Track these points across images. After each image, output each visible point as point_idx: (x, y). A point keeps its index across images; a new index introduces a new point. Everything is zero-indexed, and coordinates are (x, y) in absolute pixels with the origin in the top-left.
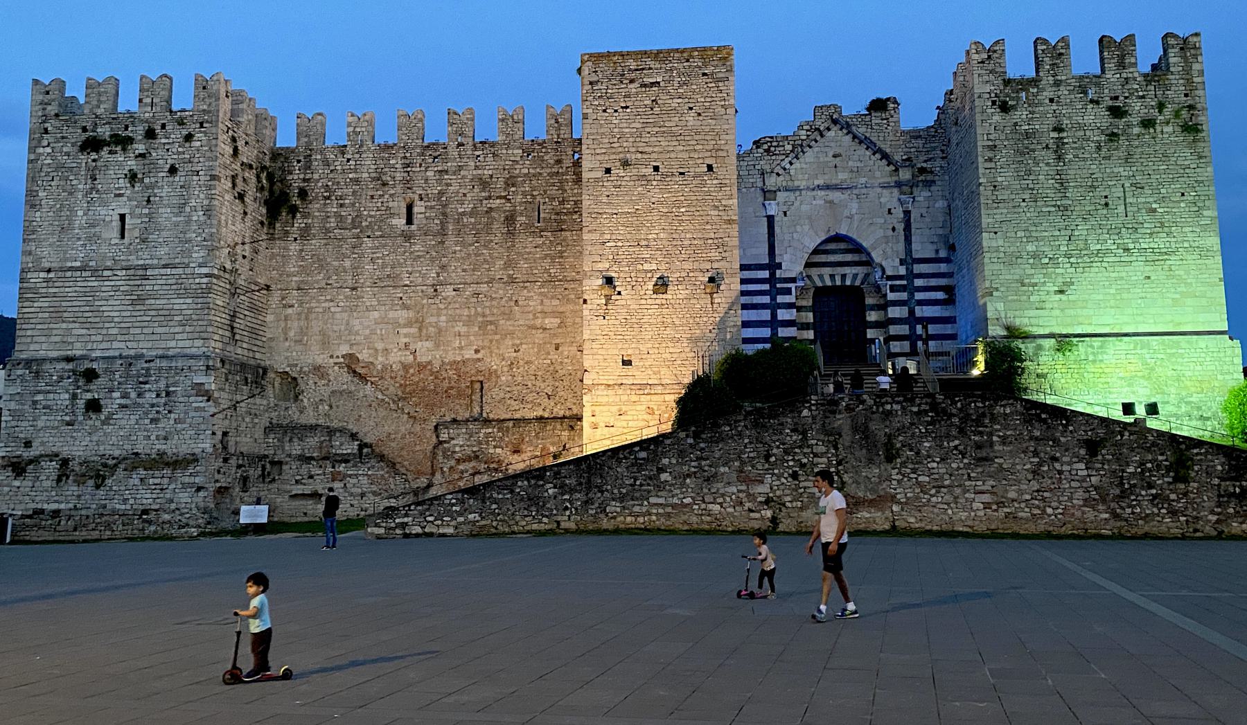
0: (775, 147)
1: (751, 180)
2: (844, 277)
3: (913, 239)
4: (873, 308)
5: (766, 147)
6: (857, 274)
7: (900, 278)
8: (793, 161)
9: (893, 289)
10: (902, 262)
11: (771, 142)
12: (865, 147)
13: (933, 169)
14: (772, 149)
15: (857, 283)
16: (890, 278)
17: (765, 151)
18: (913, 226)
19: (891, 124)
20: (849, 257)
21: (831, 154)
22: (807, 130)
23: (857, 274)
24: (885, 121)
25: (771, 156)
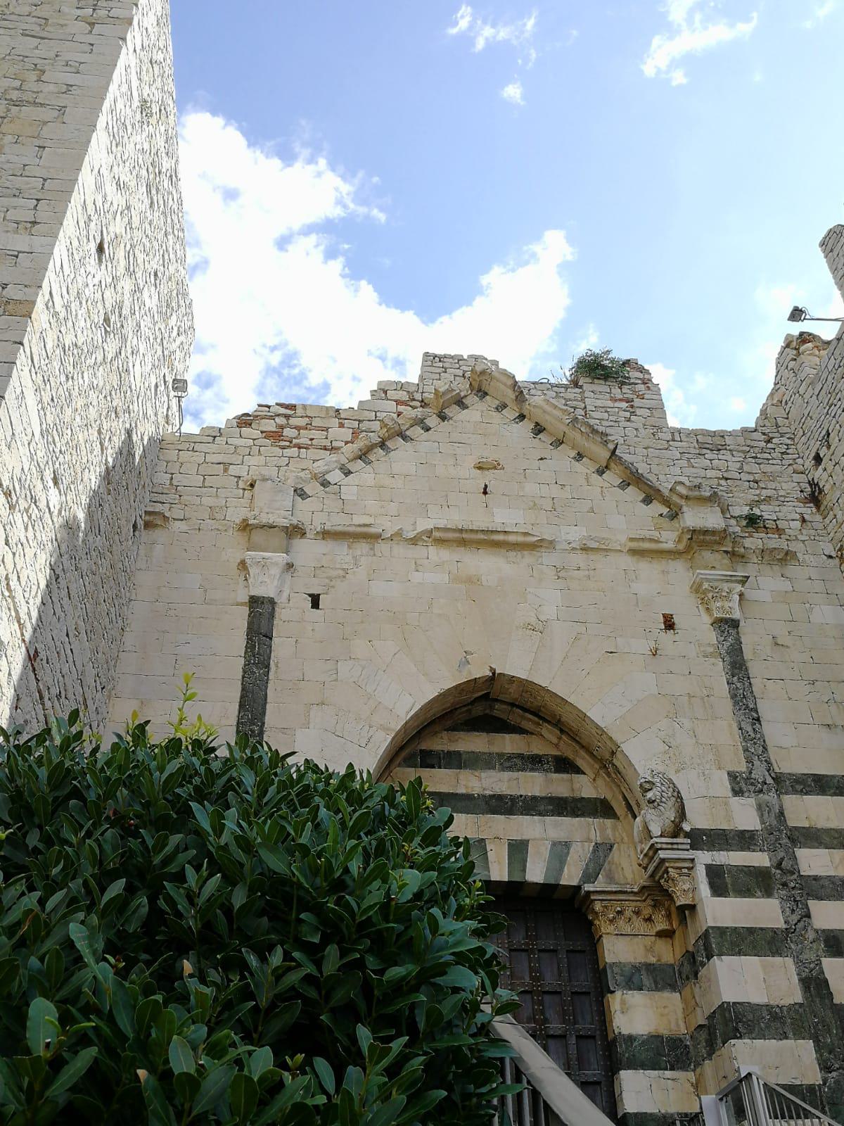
0: (298, 428)
1: (207, 501)
2: (518, 850)
3: (764, 709)
4: (637, 977)
5: (270, 426)
6: (567, 845)
7: (745, 840)
8: (350, 466)
9: (720, 881)
10: (739, 784)
11: (287, 417)
12: (573, 453)
13: (781, 524)
14: (288, 432)
15: (570, 876)
16: (699, 839)
17: (267, 435)
18: (755, 669)
19: (638, 412)
20: (533, 784)
21: (471, 461)
22: (398, 402)
23: (567, 845)
24: (624, 405)
25: (283, 448)
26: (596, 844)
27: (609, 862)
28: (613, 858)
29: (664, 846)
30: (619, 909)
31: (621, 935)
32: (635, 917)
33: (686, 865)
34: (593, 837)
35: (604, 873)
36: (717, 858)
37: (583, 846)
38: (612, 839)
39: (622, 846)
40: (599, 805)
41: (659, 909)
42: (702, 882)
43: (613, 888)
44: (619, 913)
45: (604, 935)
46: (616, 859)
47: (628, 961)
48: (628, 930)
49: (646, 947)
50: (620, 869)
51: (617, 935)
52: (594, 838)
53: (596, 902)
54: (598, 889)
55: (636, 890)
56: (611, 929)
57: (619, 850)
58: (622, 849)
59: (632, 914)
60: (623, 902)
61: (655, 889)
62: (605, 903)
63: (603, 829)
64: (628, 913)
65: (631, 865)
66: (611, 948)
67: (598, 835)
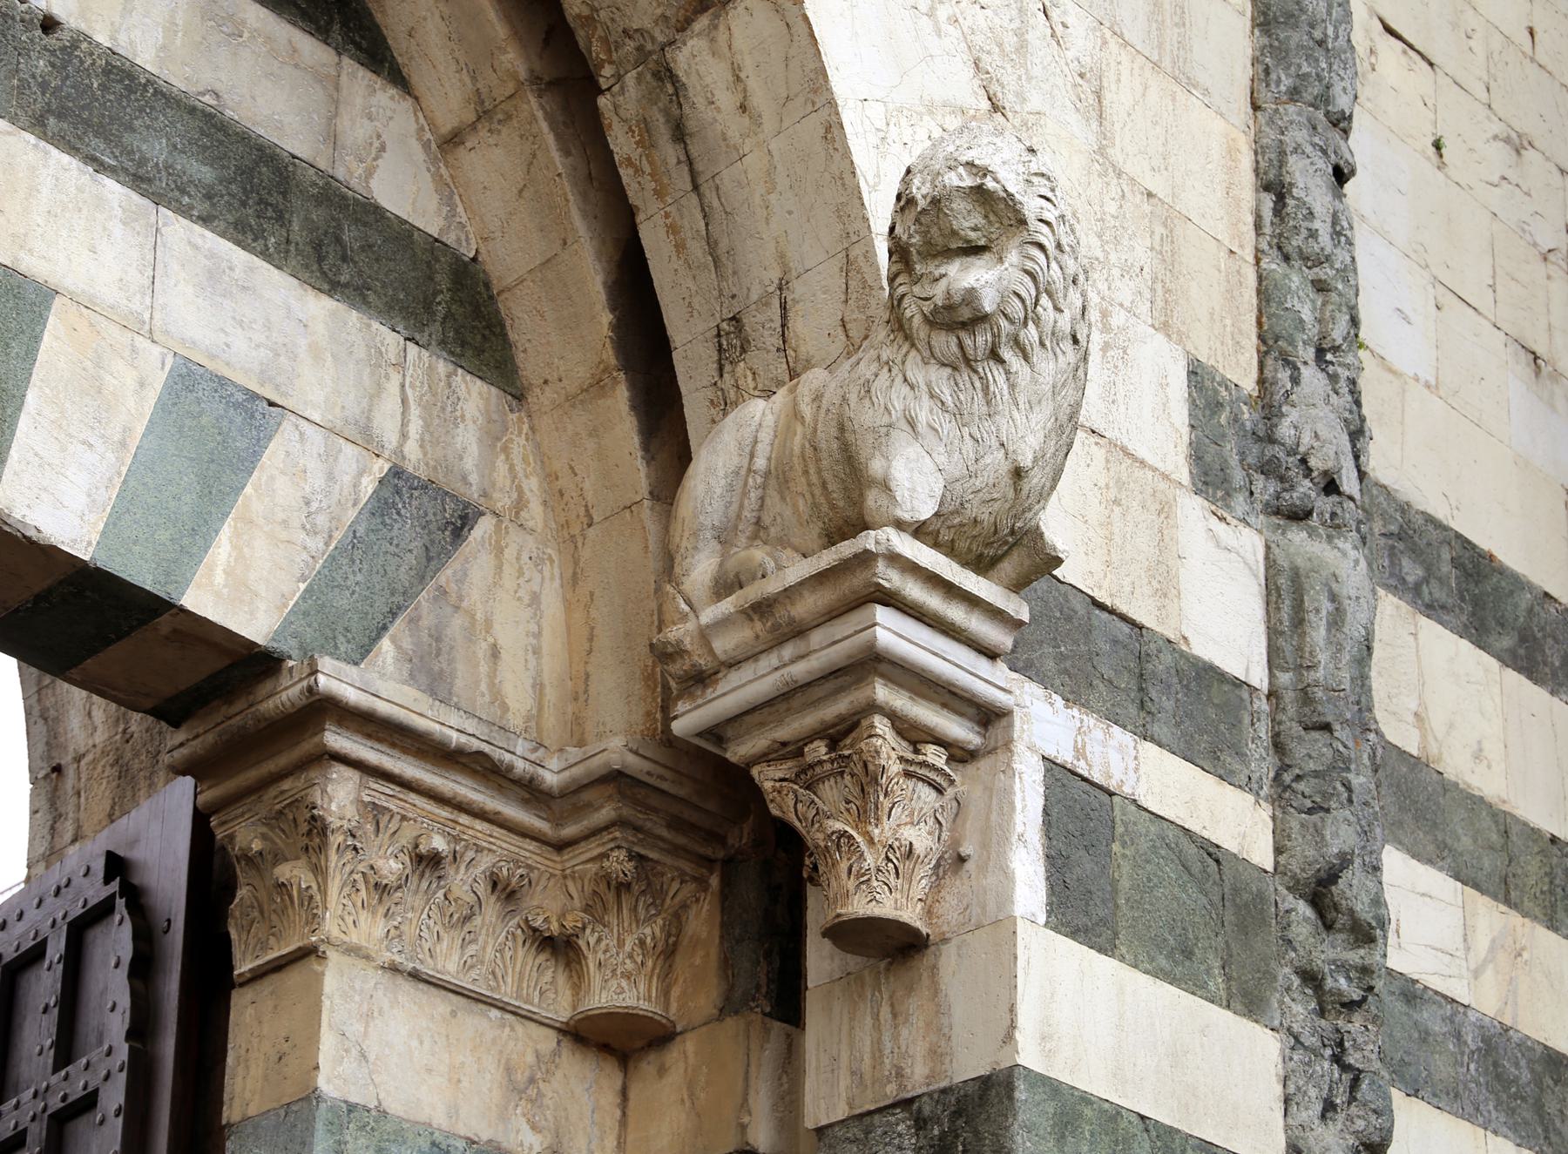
26: (397, 472)
27: (443, 592)
28: (462, 578)
29: (915, 591)
30: (439, 843)
31: (415, 976)
32: (491, 909)
33: (958, 729)
34: (387, 427)
35: (407, 644)
36: (1094, 750)
37: (330, 456)
38: (474, 478)
39: (514, 539)
40: (443, 281)
41: (634, 909)
42: (1021, 836)
43: (449, 726)
44: (428, 862)
45: (332, 955)
46: (474, 596)
47: (422, 1117)
48: (448, 964)
49: (509, 1070)
50: (482, 648)
51: (394, 969)
52: (391, 438)
53: (339, 772)
54: (383, 708)
55: (551, 778)
56: (369, 929)
57: (499, 551)
58: (510, 553)
59: (482, 889)
60: (464, 819)
61: (654, 801)
62: (380, 792)
63: (441, 415)
64: (463, 881)
65: (537, 652)
66: (354, 1029)
67: (415, 428)
